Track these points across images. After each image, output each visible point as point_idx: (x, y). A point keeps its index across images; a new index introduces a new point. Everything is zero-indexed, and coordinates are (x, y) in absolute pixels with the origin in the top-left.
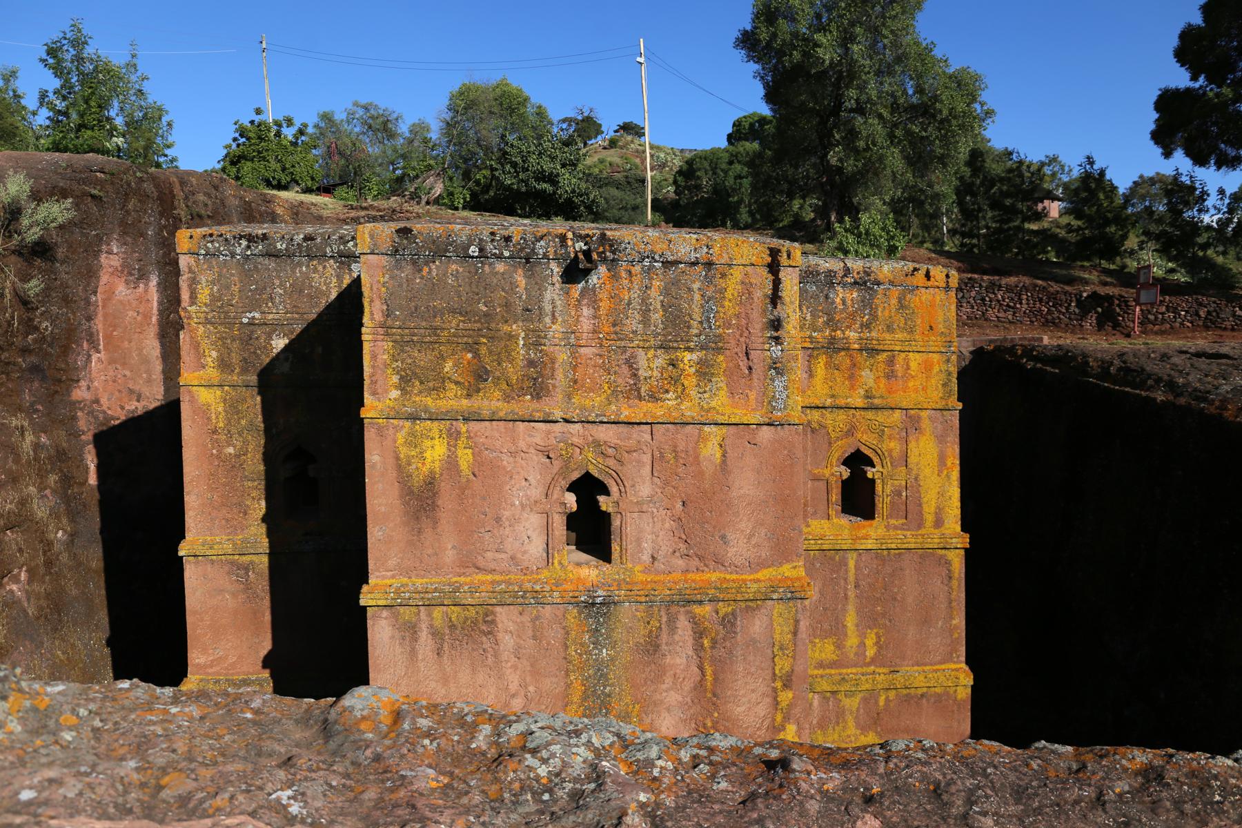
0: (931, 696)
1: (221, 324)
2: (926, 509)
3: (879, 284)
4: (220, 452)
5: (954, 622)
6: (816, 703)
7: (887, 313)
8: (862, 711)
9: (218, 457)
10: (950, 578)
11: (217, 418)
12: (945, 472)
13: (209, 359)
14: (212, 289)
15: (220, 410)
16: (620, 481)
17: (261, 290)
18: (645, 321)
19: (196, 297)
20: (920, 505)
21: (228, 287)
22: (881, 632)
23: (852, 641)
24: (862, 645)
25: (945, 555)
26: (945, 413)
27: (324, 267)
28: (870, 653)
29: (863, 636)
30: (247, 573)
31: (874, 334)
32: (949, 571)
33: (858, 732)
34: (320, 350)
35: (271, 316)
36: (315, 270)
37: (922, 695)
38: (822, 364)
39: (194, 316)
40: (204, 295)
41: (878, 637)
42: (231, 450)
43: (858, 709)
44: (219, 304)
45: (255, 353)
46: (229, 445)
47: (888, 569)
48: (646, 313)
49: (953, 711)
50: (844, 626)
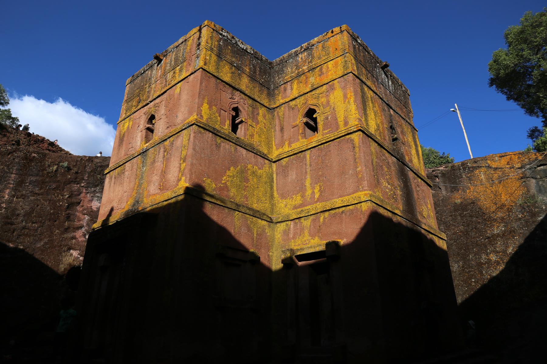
0: (347, 211)
2: (339, 120)
3: (313, 45)
5: (358, 169)
6: (292, 226)
7: (318, 54)
8: (312, 226)
10: (354, 147)
12: (347, 101)
20: (337, 119)
22: (321, 184)
23: (309, 192)
24: (313, 193)
25: (351, 137)
26: (345, 77)
28: (317, 196)
29: (313, 188)
31: (313, 63)
32: (353, 144)
33: (310, 238)
37: (342, 212)
38: (296, 84)
41: (320, 187)
43: (310, 226)
47: (324, 153)
49: (361, 218)
50: (305, 186)
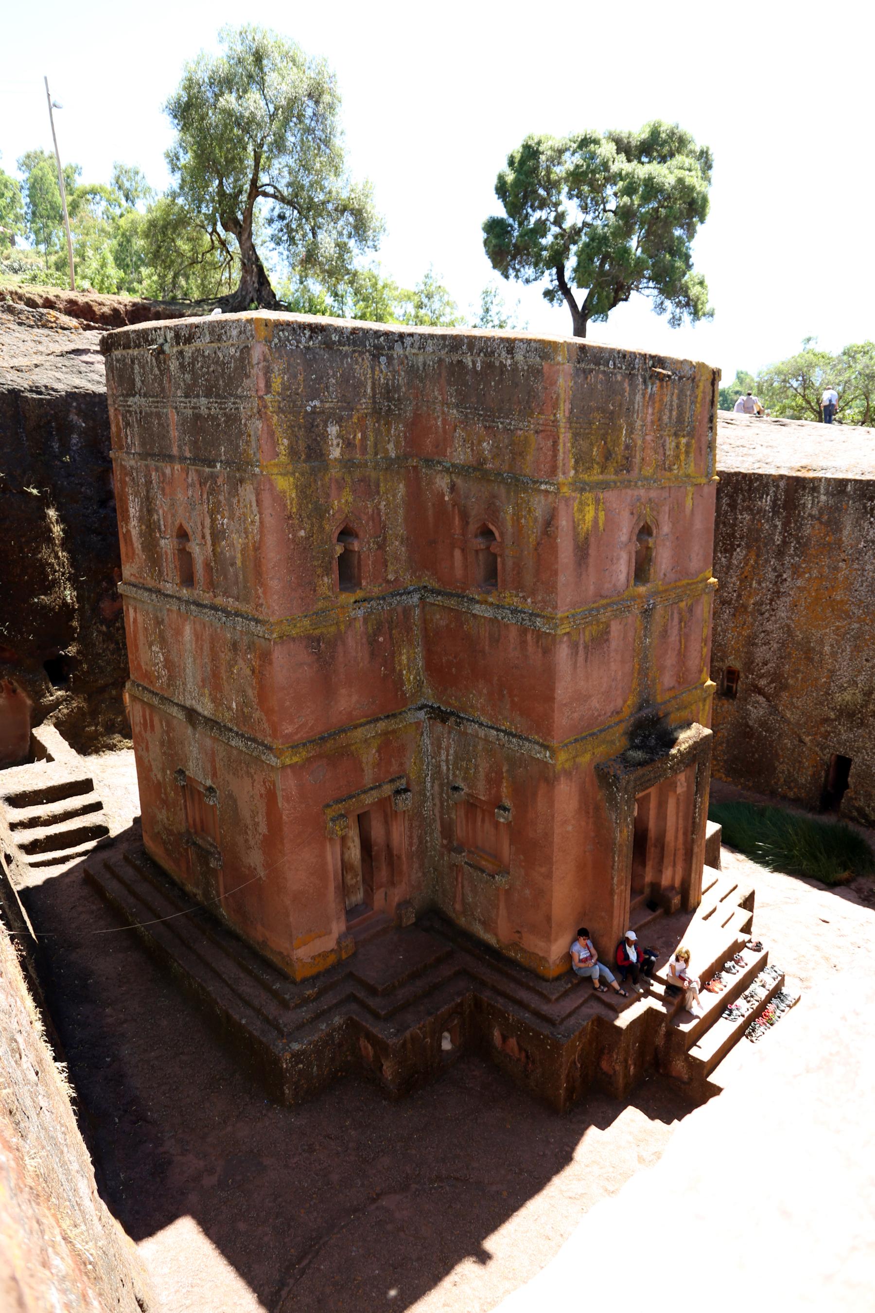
1: (290, 413)
4: (294, 536)
9: (294, 541)
11: (291, 504)
13: (282, 448)
14: (283, 378)
15: (294, 495)
16: (657, 526)
17: (319, 379)
18: (670, 418)
19: (271, 386)
21: (295, 377)
27: (363, 359)
30: (319, 644)
34: (359, 435)
35: (327, 405)
36: (357, 363)
39: (269, 404)
40: (277, 385)
42: (302, 533)
44: (288, 393)
45: (316, 440)
46: (301, 528)
48: (671, 411)
